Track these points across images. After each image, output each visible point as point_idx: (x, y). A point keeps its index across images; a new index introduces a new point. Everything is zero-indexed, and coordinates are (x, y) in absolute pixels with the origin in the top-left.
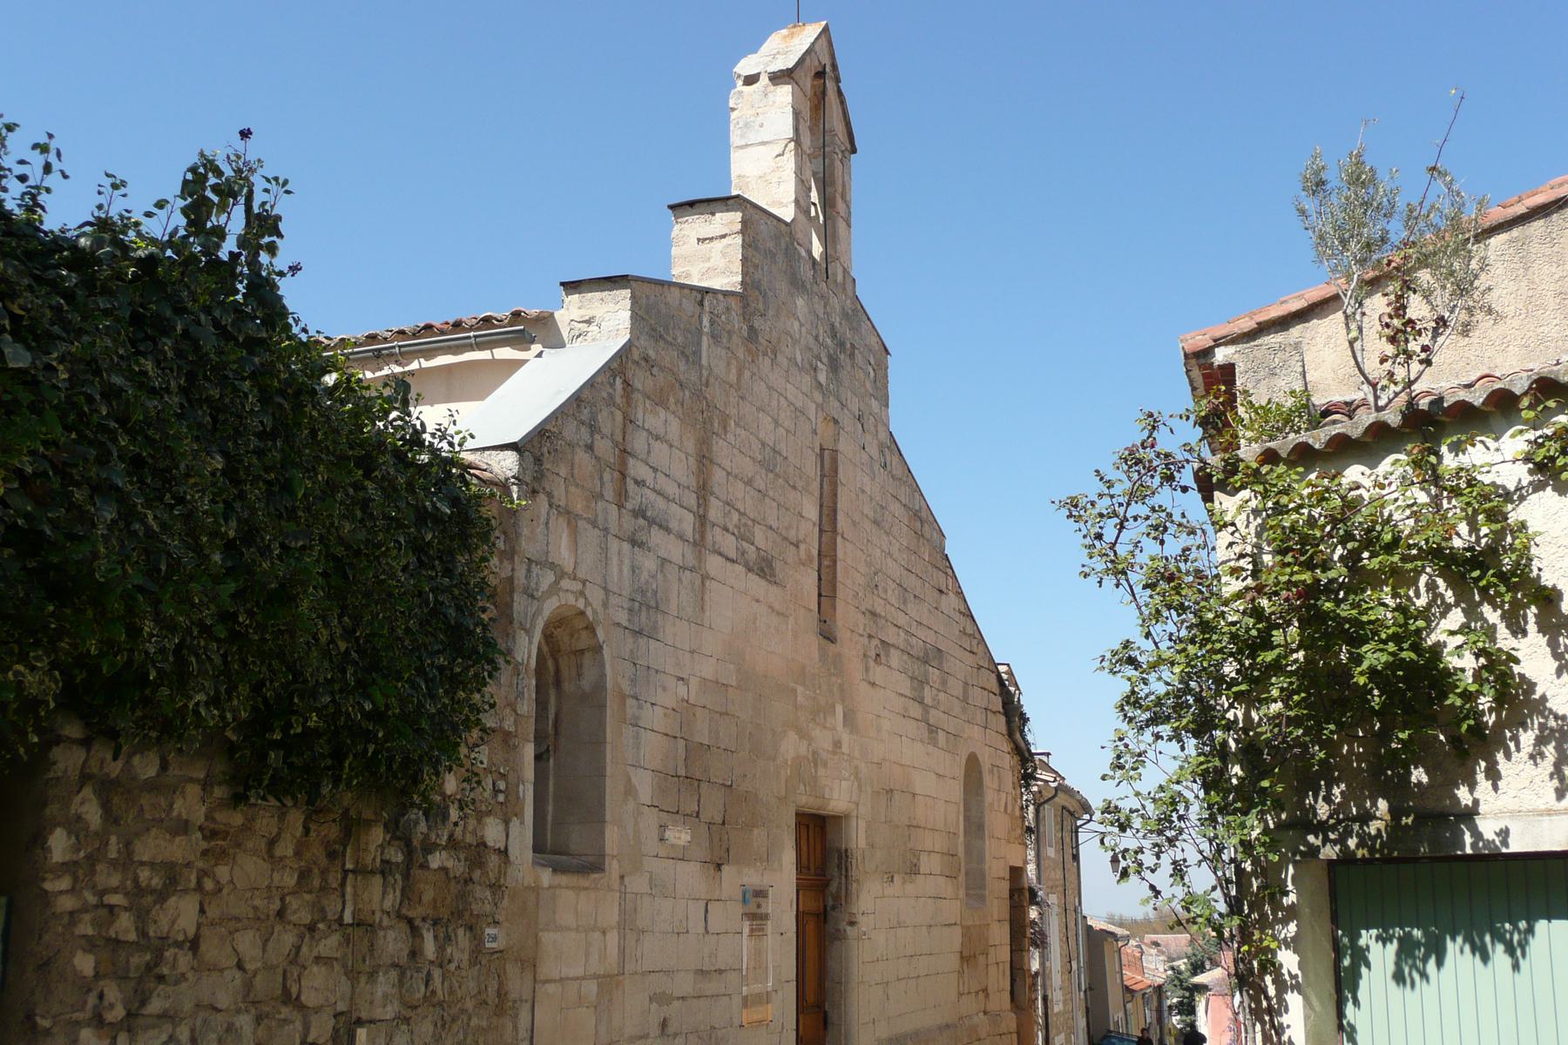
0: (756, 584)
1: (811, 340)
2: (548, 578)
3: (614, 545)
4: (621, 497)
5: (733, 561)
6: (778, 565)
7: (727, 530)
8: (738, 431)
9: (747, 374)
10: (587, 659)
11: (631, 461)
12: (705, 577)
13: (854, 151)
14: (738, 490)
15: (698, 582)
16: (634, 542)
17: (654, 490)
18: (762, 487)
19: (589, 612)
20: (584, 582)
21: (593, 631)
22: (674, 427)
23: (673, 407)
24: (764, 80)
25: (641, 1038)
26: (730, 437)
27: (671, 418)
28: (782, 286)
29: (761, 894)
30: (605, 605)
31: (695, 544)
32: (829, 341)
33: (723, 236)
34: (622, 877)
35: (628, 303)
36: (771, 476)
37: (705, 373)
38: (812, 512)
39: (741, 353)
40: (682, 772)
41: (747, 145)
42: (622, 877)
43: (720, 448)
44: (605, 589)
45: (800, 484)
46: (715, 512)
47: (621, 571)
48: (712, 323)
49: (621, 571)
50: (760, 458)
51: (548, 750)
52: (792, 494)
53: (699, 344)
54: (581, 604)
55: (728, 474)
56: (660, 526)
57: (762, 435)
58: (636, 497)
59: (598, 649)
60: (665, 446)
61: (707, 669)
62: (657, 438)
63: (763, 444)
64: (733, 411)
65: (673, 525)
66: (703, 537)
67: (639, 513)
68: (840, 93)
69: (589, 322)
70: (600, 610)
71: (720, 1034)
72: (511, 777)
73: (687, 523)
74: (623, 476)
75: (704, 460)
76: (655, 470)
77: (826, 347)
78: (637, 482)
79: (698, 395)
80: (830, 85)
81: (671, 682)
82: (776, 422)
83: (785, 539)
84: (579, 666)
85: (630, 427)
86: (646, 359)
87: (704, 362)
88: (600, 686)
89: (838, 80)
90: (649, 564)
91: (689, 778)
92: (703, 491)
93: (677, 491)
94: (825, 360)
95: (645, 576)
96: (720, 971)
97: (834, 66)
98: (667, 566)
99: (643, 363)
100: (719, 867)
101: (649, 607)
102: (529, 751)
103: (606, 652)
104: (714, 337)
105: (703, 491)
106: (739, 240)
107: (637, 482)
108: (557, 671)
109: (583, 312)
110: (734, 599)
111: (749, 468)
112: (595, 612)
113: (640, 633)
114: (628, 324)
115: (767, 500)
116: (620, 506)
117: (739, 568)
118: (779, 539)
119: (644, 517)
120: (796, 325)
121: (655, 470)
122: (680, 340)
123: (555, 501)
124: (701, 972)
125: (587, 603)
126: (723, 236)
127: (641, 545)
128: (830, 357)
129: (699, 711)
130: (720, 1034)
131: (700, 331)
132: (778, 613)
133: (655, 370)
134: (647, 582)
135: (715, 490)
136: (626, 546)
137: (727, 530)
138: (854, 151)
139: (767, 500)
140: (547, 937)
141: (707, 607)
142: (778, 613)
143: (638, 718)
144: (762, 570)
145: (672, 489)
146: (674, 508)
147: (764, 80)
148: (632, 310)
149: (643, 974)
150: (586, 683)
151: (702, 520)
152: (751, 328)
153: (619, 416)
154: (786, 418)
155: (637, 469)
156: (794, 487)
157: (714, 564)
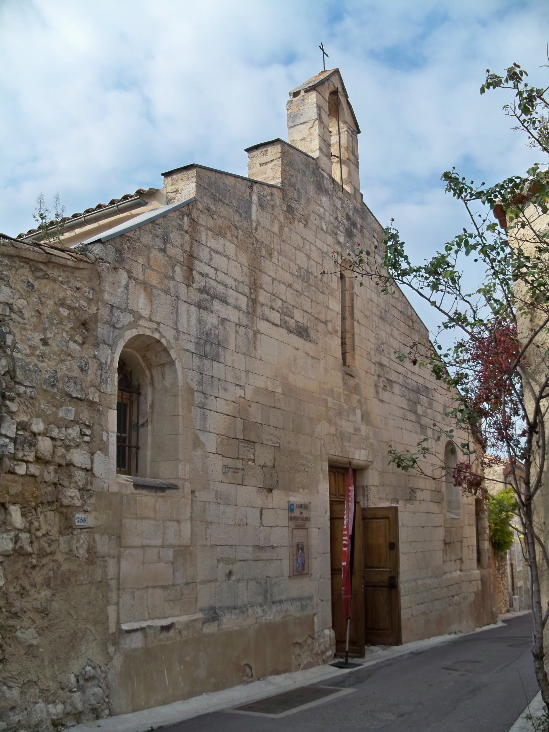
0: (295, 340)
1: (332, 219)
2: (127, 319)
3: (183, 307)
4: (189, 281)
5: (277, 325)
6: (312, 333)
7: (273, 309)
8: (280, 257)
9: (286, 229)
10: (167, 370)
11: (196, 262)
12: (256, 333)
13: (359, 132)
14: (282, 289)
15: (251, 334)
16: (199, 306)
17: (215, 280)
18: (299, 289)
19: (163, 341)
20: (158, 324)
21: (168, 353)
22: (231, 249)
23: (229, 238)
24: (302, 93)
25: (210, 581)
26: (275, 260)
27: (228, 244)
28: (312, 190)
29: (305, 507)
30: (177, 338)
31: (248, 313)
32: (345, 222)
33: (272, 161)
34: (193, 492)
35: (194, 179)
36: (305, 284)
37: (254, 224)
38: (336, 306)
39: (282, 218)
40: (240, 436)
41: (295, 126)
42: (193, 492)
43: (267, 265)
44: (177, 329)
45: (326, 291)
46: (263, 297)
47: (189, 321)
48: (259, 199)
49: (189, 321)
50: (297, 274)
51: (147, 421)
52: (321, 296)
53: (250, 208)
54: (157, 336)
55: (274, 279)
56: (221, 300)
57: (298, 262)
58: (199, 281)
59: (172, 363)
60: (225, 259)
61: (261, 383)
62: (217, 253)
63: (300, 267)
64: (277, 247)
65: (231, 300)
66: (254, 310)
67: (203, 291)
68: (348, 103)
69: (176, 191)
70: (173, 342)
71: (274, 581)
72: (96, 427)
73: (243, 302)
74: (191, 270)
75: (255, 270)
76: (217, 270)
77: (343, 224)
78: (201, 274)
79: (249, 234)
80: (342, 99)
81: (231, 387)
82: (309, 258)
83: (317, 319)
84: (163, 374)
85: (195, 244)
86: (209, 210)
87: (254, 217)
88: (175, 384)
89: (346, 97)
90: (211, 320)
91: (243, 438)
92: (255, 286)
93: (234, 283)
94: (343, 230)
95: (209, 326)
96: (273, 547)
97: (344, 90)
98: (227, 323)
99: (206, 212)
100: (270, 490)
101: (212, 344)
102: (113, 416)
103: (178, 365)
104: (262, 206)
105: (255, 286)
106: (280, 161)
107: (201, 274)
108: (152, 377)
109: (173, 187)
110: (276, 345)
111: (288, 278)
112: (168, 342)
113: (206, 356)
114: (194, 189)
115: (302, 296)
116: (188, 286)
117: (283, 331)
118: (312, 319)
119: (208, 293)
120: (322, 210)
121: (217, 270)
122: (235, 203)
123: (134, 275)
124: (259, 548)
125: (162, 336)
126: (272, 161)
127: (206, 309)
128: (346, 230)
129: (253, 405)
130: (274, 581)
131: (250, 202)
132: (313, 357)
133: (215, 217)
134: (210, 330)
135: (264, 286)
136: (193, 309)
137: (273, 309)
138: (359, 132)
139: (302, 296)
140: (127, 522)
141: (258, 348)
142: (313, 357)
143: (205, 404)
144: (300, 333)
145: (230, 282)
146: (231, 292)
147: (302, 93)
148: (197, 183)
149: (212, 546)
150: (167, 384)
151: (254, 301)
152: (289, 206)
153: (187, 237)
154: (315, 255)
155: (199, 266)
156: (323, 293)
157: (263, 326)
